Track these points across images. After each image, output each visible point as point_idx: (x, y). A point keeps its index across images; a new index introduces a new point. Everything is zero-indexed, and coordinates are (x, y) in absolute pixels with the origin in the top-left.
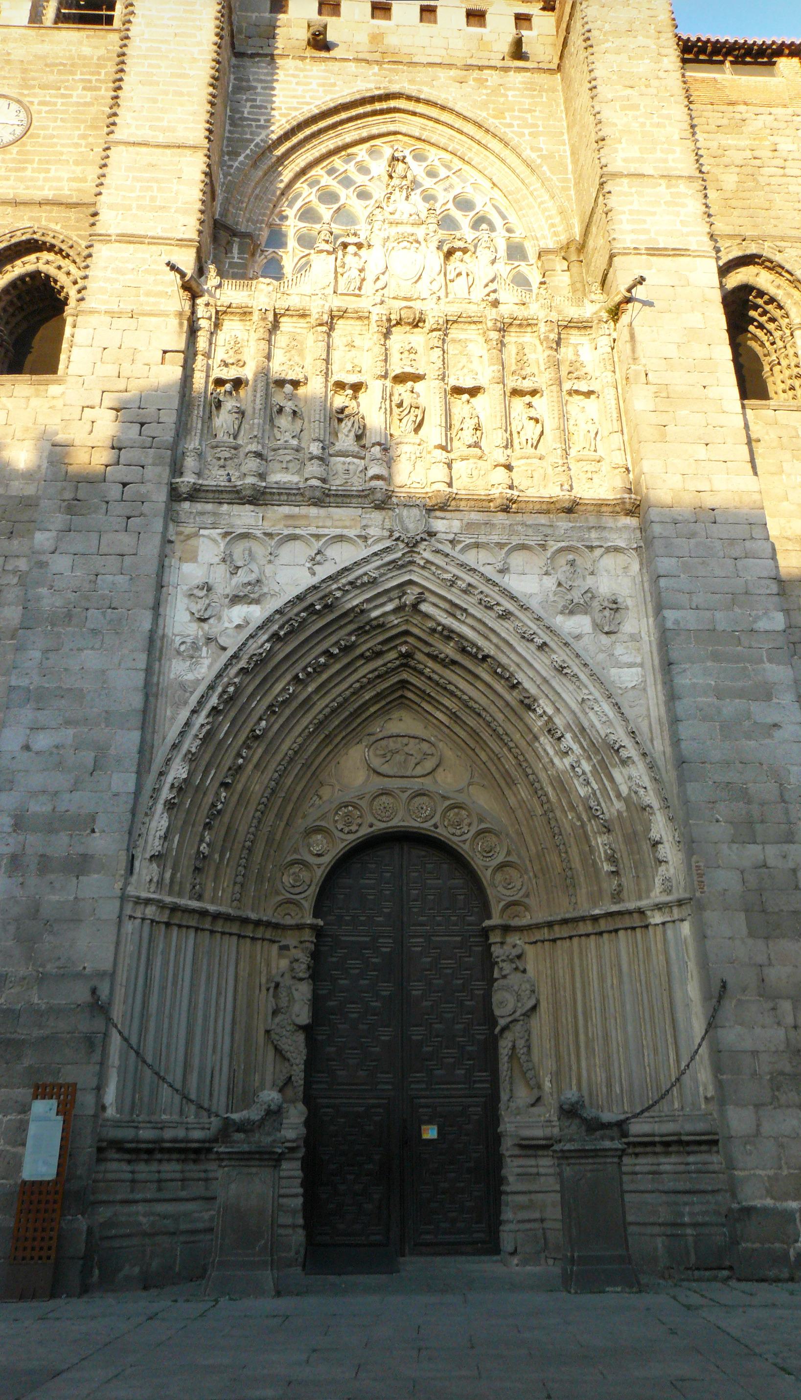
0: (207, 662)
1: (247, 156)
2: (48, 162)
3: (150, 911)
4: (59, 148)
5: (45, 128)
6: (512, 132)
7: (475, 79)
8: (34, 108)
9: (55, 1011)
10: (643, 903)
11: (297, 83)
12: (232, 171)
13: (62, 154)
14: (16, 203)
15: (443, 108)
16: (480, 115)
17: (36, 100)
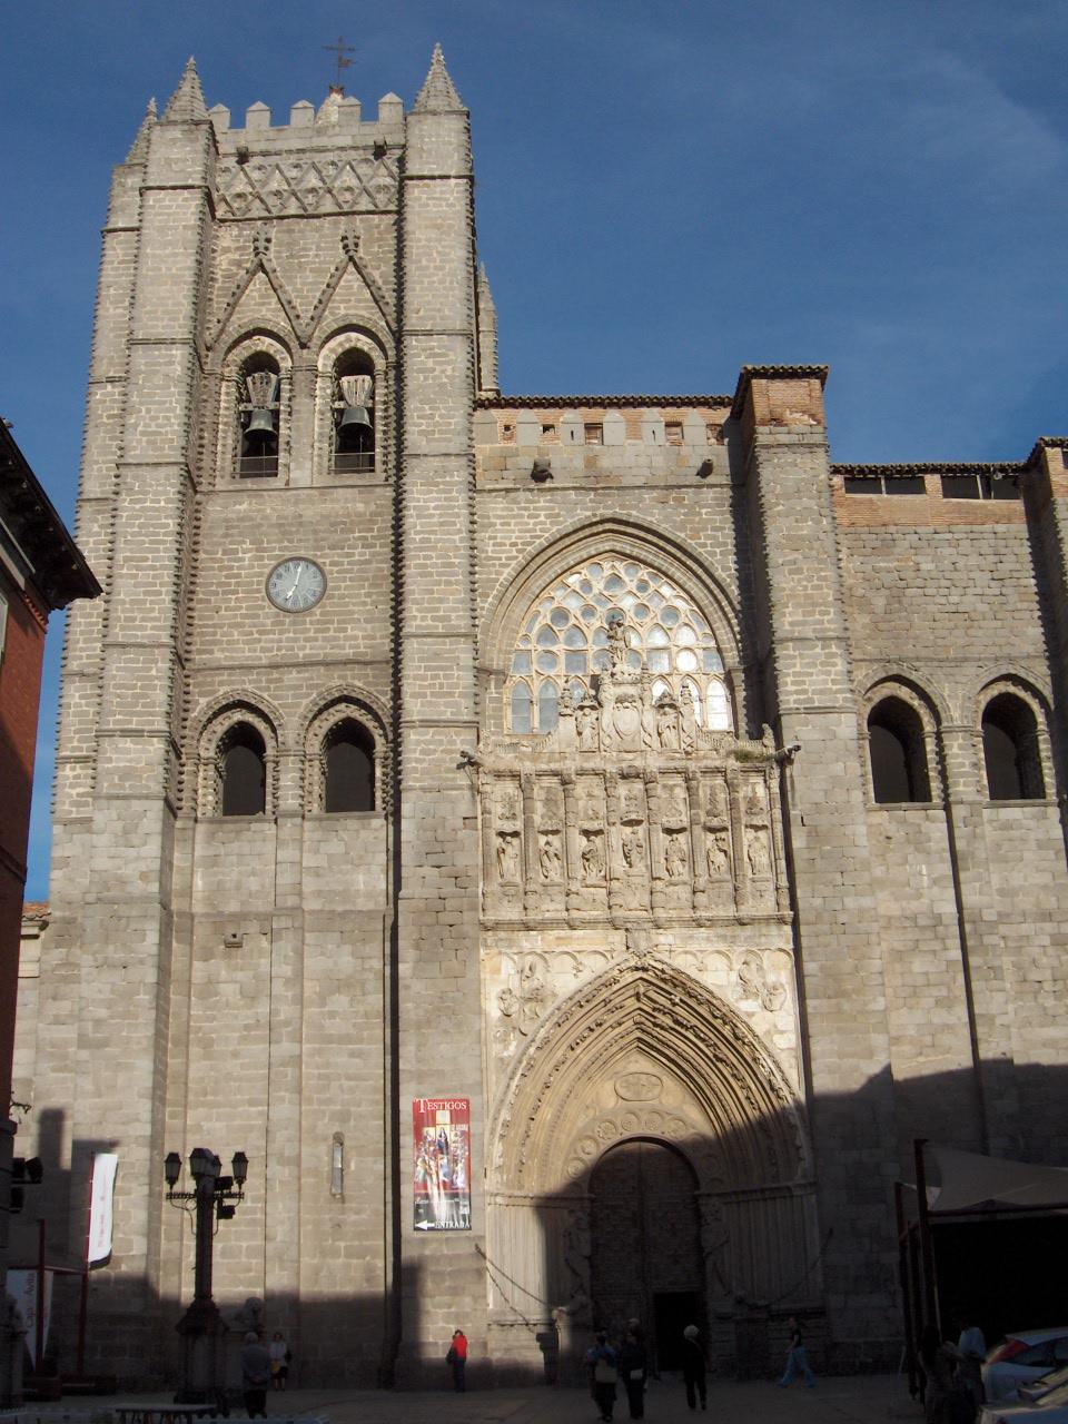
0: (514, 1043)
1: (495, 596)
2: (344, 622)
3: (499, 1200)
4: (351, 607)
5: (338, 588)
6: (706, 552)
7: (675, 499)
8: (327, 568)
9: (458, 1257)
10: (790, 1184)
11: (528, 517)
12: (484, 613)
13: (353, 612)
14: (326, 664)
15: (648, 530)
16: (680, 536)
17: (328, 561)
